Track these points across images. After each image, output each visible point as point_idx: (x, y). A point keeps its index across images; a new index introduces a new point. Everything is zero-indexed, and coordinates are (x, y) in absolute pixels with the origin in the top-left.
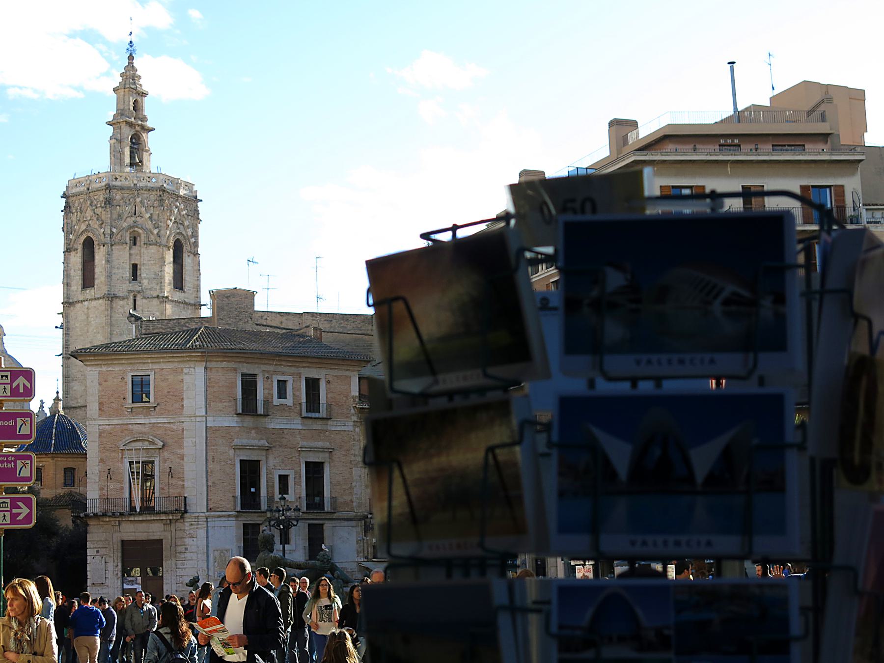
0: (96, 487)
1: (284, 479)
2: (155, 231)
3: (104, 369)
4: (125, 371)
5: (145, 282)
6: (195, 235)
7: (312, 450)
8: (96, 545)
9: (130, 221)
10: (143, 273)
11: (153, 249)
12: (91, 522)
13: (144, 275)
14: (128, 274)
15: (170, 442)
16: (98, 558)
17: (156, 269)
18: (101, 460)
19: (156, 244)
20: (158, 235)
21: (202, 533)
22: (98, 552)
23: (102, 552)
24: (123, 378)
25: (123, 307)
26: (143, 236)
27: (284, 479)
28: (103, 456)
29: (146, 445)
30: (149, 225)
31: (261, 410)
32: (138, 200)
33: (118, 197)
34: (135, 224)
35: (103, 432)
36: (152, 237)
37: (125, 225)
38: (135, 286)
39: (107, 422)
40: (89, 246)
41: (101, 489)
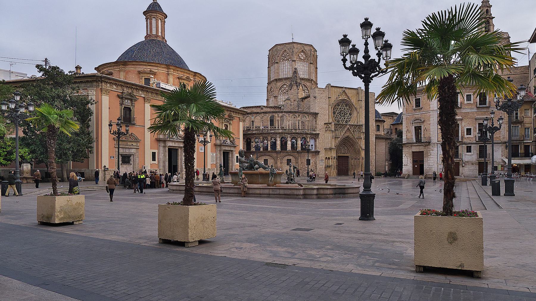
1: (469, 131)
7: (481, 119)
15: (426, 119)
21: (436, 149)
27: (469, 131)
29: (419, 121)
31: (459, 106)
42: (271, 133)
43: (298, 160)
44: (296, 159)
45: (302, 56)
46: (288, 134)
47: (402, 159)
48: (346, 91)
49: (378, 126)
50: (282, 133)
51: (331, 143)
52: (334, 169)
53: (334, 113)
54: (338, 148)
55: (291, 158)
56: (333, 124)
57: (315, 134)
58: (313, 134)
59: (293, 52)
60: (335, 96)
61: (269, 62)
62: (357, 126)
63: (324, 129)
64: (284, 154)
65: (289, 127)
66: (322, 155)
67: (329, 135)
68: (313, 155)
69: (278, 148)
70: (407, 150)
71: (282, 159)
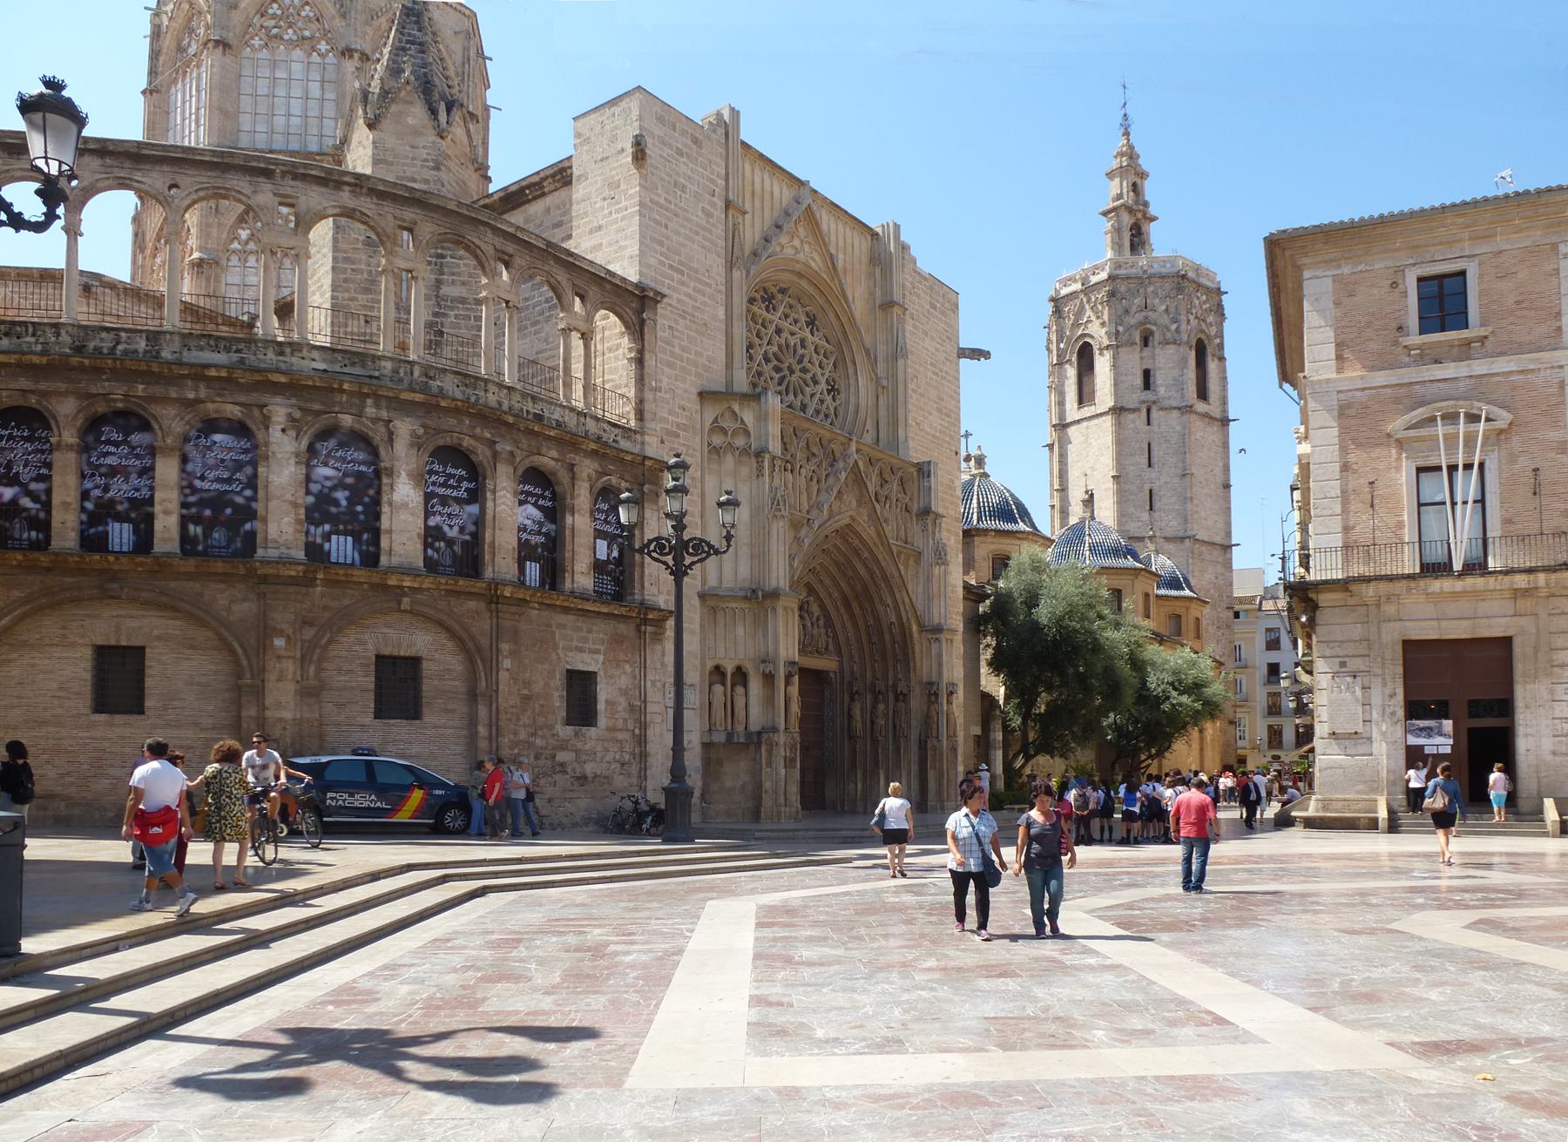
2: (1174, 327)
5: (1162, 390)
6: (1220, 335)
9: (1140, 317)
10: (1159, 379)
11: (1172, 349)
13: (1159, 382)
14: (1139, 381)
17: (1176, 372)
19: (1175, 343)
20: (1177, 330)
25: (1134, 421)
26: (1157, 335)
30: (1165, 320)
32: (1151, 289)
33: (1123, 289)
34: (1147, 320)
36: (1168, 335)
37: (1133, 322)
38: (1148, 396)
40: (1085, 357)
43: (492, 666)
51: (760, 556)
55: (419, 641)
68: (617, 640)
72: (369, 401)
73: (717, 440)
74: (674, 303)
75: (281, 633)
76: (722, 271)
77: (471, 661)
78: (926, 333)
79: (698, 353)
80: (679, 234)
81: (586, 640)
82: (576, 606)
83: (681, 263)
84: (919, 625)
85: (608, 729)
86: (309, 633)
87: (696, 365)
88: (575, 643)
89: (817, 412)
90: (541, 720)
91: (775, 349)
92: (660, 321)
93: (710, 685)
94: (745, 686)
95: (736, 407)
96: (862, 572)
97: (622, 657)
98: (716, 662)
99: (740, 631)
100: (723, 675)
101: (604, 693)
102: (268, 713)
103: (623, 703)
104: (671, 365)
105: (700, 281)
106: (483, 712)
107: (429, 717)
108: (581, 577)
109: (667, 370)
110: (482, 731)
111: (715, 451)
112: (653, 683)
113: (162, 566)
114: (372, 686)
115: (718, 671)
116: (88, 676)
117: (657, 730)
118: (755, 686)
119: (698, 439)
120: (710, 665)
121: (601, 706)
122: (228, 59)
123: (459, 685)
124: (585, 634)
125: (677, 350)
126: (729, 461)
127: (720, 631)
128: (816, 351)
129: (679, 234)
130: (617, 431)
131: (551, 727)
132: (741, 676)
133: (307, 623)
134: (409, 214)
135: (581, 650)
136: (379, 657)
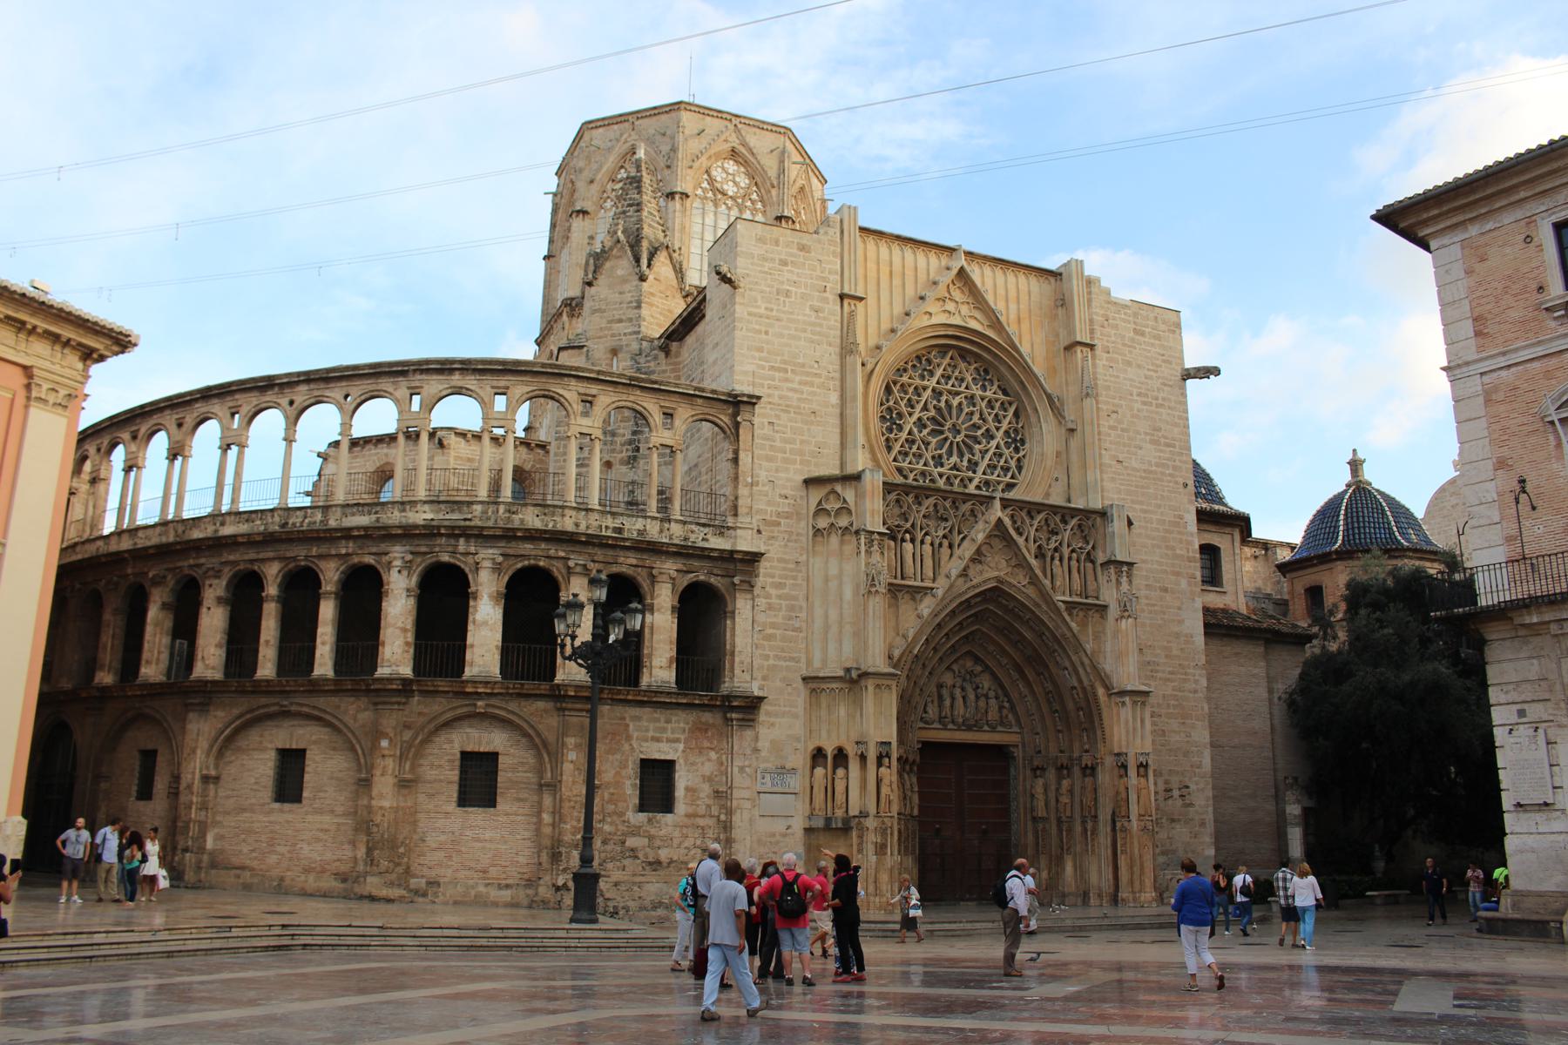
0: (1496, 534)
3: (1474, 230)
4: (1530, 221)
8: (1513, 696)
12: (1493, 632)
16: (1524, 731)
18: (1501, 464)
22: (1521, 713)
23: (1535, 712)
24: (1528, 239)
28: (1505, 452)
35: (1496, 389)
39: (1502, 361)
41: (1509, 539)
42: (346, 534)
44: (545, 750)
45: (731, 177)
46: (481, 536)
47: (1489, 748)
48: (976, 273)
49: (1210, 553)
50: (430, 532)
51: (860, 635)
52: (881, 849)
53: (891, 419)
54: (919, 676)
56: (873, 482)
57: (729, 557)
58: (703, 554)
59: (674, 150)
60: (901, 307)
61: (553, 226)
62: (1065, 513)
63: (803, 527)
64: (438, 707)
65: (496, 487)
66: (785, 729)
67: (845, 571)
68: (700, 729)
69: (396, 653)
70: (1533, 669)
71: (411, 752)
72: (462, 541)
73: (823, 523)
74: (776, 400)
75: (385, 735)
76: (836, 359)
77: (539, 756)
78: (1129, 363)
79: (802, 442)
80: (781, 335)
81: (664, 730)
82: (655, 701)
83: (785, 362)
84: (1107, 688)
85: (688, 816)
86: (407, 735)
87: (801, 453)
88: (651, 734)
89: (992, 467)
90: (611, 808)
91: (933, 413)
92: (756, 420)
93: (813, 768)
94: (846, 768)
95: (838, 488)
96: (1028, 635)
97: (706, 744)
98: (817, 743)
99: (842, 711)
100: (825, 756)
101: (682, 780)
102: (374, 803)
103: (706, 789)
104: (770, 459)
105: (808, 374)
106: (548, 801)
107: (503, 804)
108: (660, 668)
109: (765, 464)
110: (547, 818)
111: (818, 532)
112: (742, 769)
113: (317, 688)
114: (457, 778)
115: (818, 755)
116: (271, 773)
117: (746, 815)
118: (854, 766)
119: (803, 524)
120: (811, 747)
121: (680, 792)
122: (587, 221)
123: (532, 777)
124: (662, 724)
125: (778, 444)
126: (834, 540)
127: (824, 713)
128: (990, 405)
129: (781, 335)
130: (706, 530)
131: (622, 814)
132: (841, 757)
133: (407, 726)
134: (503, 381)
135: (658, 740)
136: (463, 753)
